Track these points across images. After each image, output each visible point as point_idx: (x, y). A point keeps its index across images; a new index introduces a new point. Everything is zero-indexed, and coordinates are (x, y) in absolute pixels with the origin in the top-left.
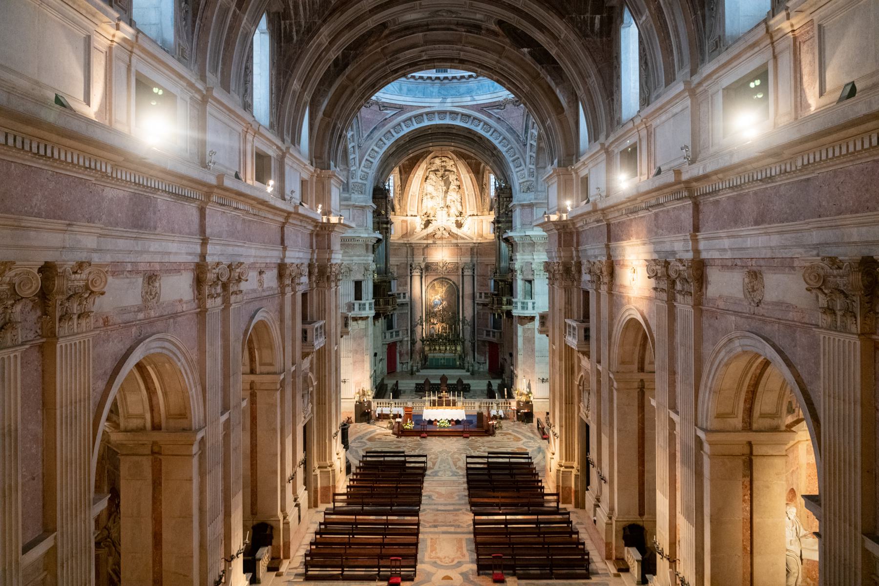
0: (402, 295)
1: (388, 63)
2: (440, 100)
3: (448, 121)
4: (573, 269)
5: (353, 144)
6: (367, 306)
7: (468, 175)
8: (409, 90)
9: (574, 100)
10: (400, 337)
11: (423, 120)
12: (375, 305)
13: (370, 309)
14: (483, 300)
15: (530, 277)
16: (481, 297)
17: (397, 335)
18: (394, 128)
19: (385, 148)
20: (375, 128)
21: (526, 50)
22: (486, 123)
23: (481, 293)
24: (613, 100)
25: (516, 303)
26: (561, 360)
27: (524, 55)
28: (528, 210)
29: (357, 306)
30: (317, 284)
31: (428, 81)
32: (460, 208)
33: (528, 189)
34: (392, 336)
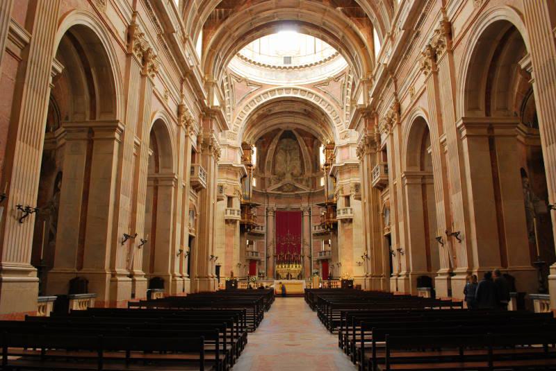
0: (260, 228)
1: (253, 19)
2: (287, 81)
3: (291, 94)
4: (375, 138)
5: (228, 98)
6: (236, 212)
7: (306, 148)
8: (266, 74)
9: (371, 26)
10: (259, 257)
11: (275, 94)
12: (241, 212)
13: (238, 214)
14: (317, 231)
15: (348, 194)
16: (315, 229)
17: (257, 255)
18: (256, 98)
19: (250, 111)
20: (244, 98)
21: (339, 8)
22: (316, 96)
23: (315, 227)
24: (393, 7)
25: (339, 210)
26: (369, 202)
27: (339, 12)
28: (345, 150)
29: (229, 211)
30: (202, 151)
31: (279, 69)
32: (301, 171)
33: (346, 136)
34: (253, 255)
